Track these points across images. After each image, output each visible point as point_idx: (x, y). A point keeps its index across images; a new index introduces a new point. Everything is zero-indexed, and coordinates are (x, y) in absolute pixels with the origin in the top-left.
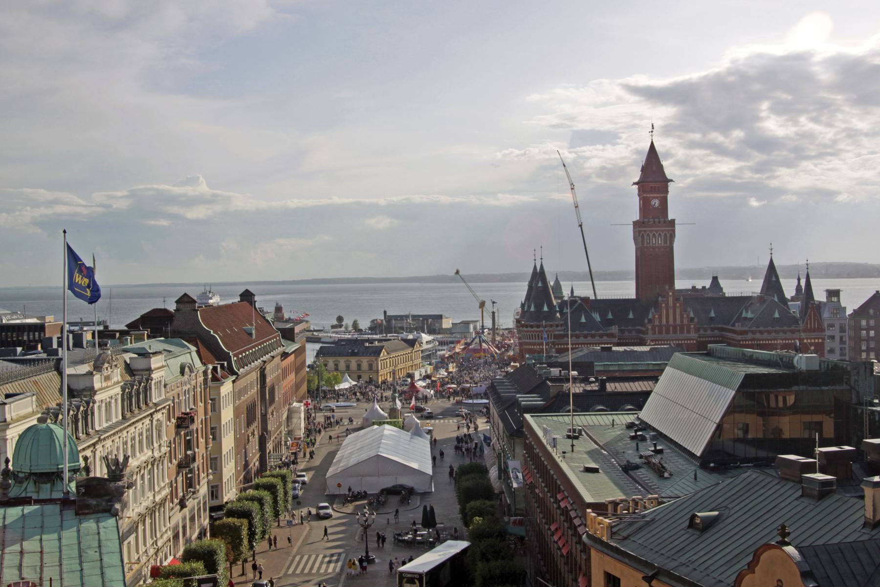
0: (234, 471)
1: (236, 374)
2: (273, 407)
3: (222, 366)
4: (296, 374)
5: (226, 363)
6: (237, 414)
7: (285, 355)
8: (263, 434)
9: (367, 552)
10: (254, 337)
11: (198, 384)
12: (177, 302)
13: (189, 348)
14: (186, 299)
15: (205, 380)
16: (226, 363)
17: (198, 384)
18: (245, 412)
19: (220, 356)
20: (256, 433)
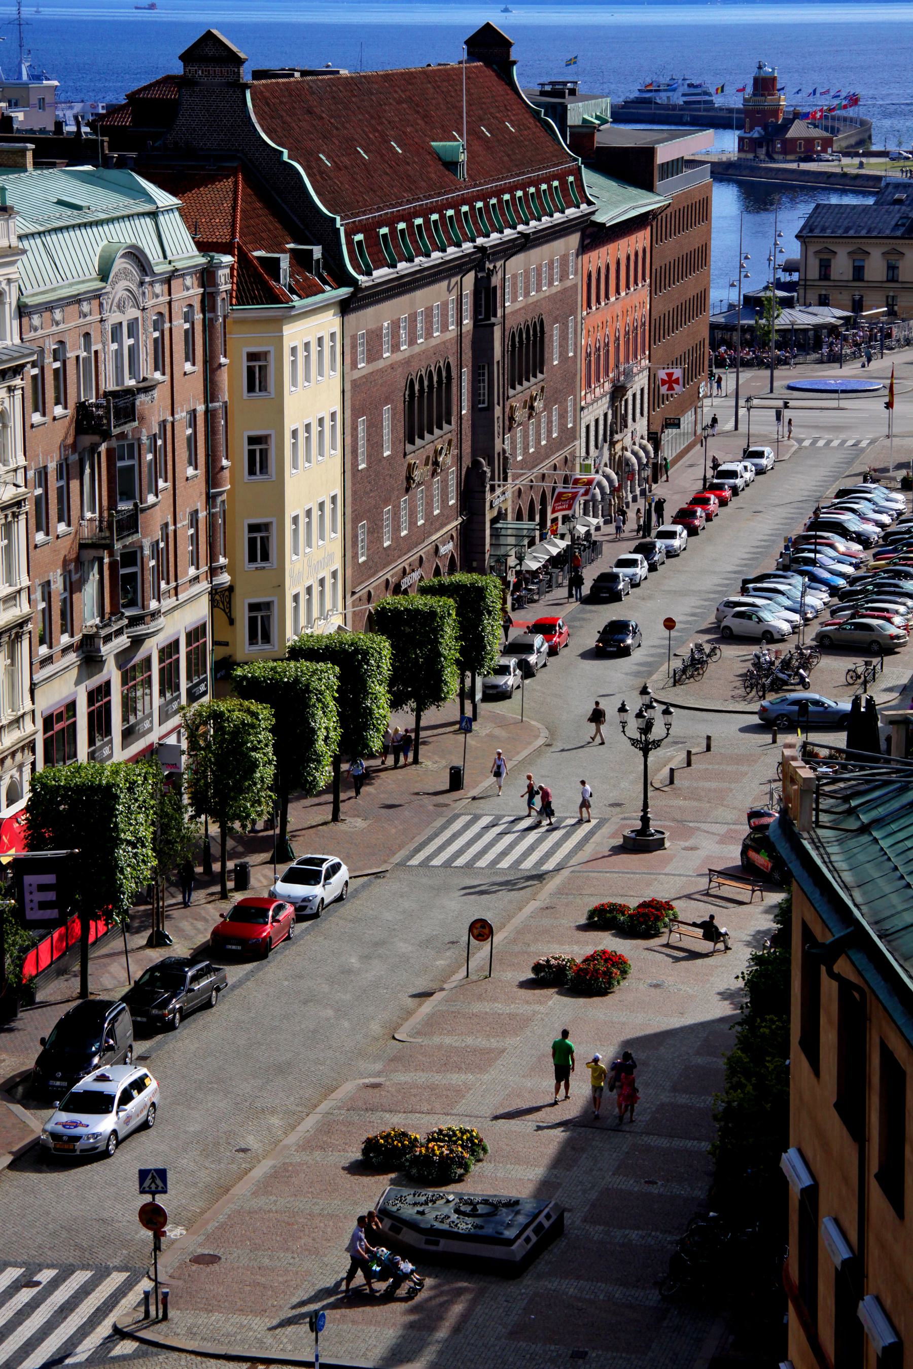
0: (337, 565)
1: (353, 282)
2: (531, 386)
3: (301, 260)
4: (654, 290)
5: (317, 252)
6: (360, 400)
7: (594, 235)
8: (476, 464)
9: (645, 820)
10: (463, 173)
11: (179, 309)
12: (186, 57)
13: (151, 200)
14: (210, 51)
15: (208, 302)
16: (317, 252)
17: (179, 309)
18: (399, 397)
19: (306, 225)
20: (447, 459)
